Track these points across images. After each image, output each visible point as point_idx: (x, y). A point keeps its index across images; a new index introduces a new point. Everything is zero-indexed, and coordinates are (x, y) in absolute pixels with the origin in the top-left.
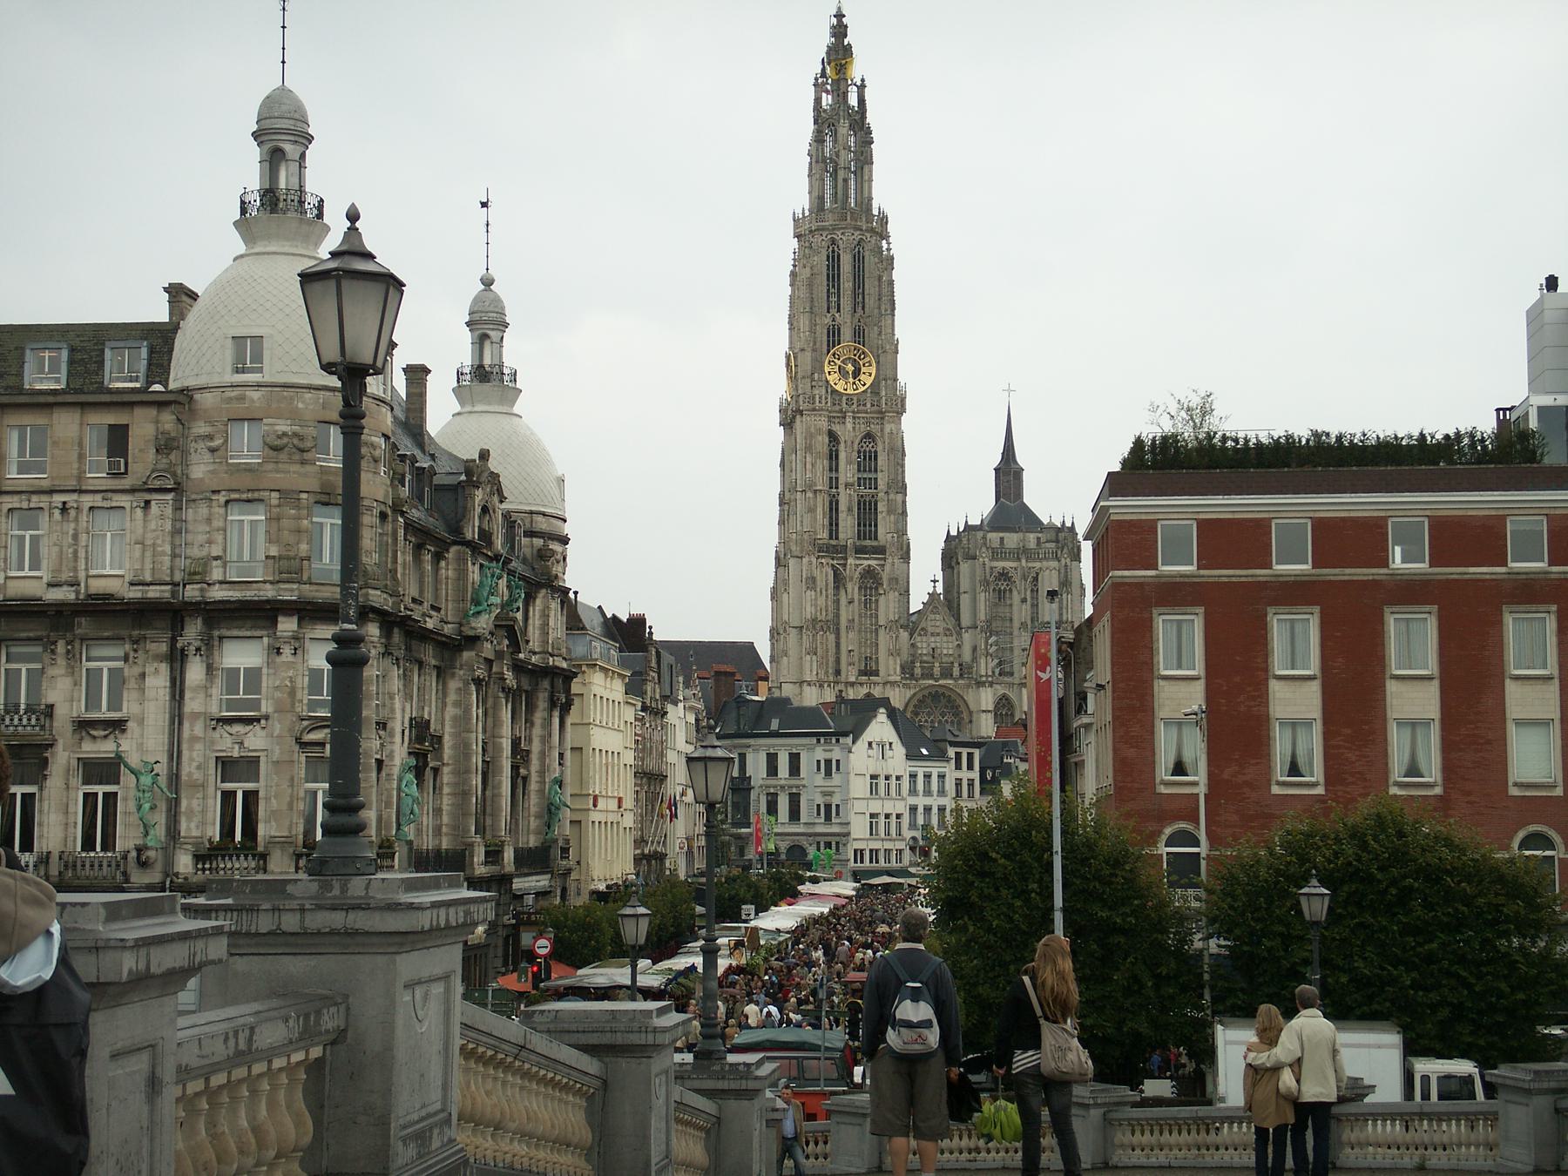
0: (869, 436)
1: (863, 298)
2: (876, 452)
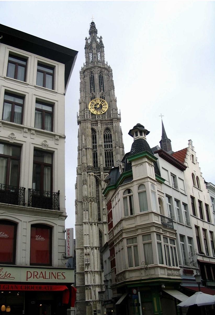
0: (107, 129)
1: (103, 88)
2: (111, 135)
